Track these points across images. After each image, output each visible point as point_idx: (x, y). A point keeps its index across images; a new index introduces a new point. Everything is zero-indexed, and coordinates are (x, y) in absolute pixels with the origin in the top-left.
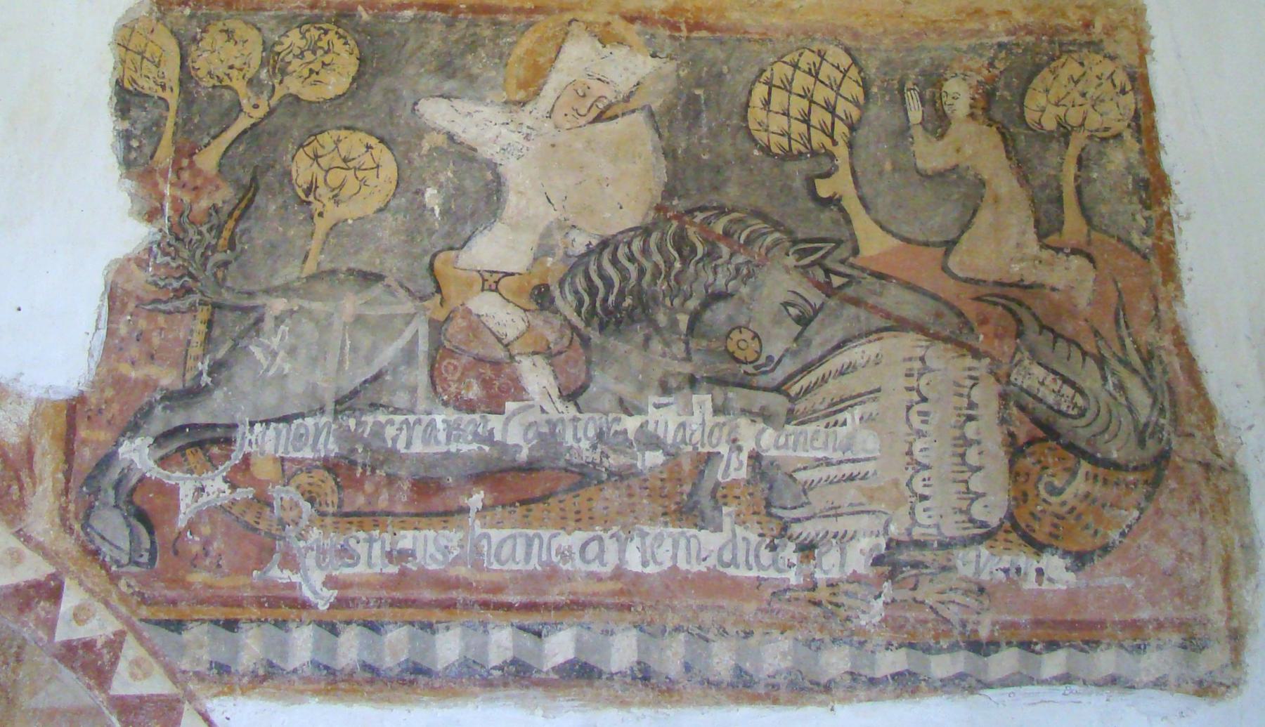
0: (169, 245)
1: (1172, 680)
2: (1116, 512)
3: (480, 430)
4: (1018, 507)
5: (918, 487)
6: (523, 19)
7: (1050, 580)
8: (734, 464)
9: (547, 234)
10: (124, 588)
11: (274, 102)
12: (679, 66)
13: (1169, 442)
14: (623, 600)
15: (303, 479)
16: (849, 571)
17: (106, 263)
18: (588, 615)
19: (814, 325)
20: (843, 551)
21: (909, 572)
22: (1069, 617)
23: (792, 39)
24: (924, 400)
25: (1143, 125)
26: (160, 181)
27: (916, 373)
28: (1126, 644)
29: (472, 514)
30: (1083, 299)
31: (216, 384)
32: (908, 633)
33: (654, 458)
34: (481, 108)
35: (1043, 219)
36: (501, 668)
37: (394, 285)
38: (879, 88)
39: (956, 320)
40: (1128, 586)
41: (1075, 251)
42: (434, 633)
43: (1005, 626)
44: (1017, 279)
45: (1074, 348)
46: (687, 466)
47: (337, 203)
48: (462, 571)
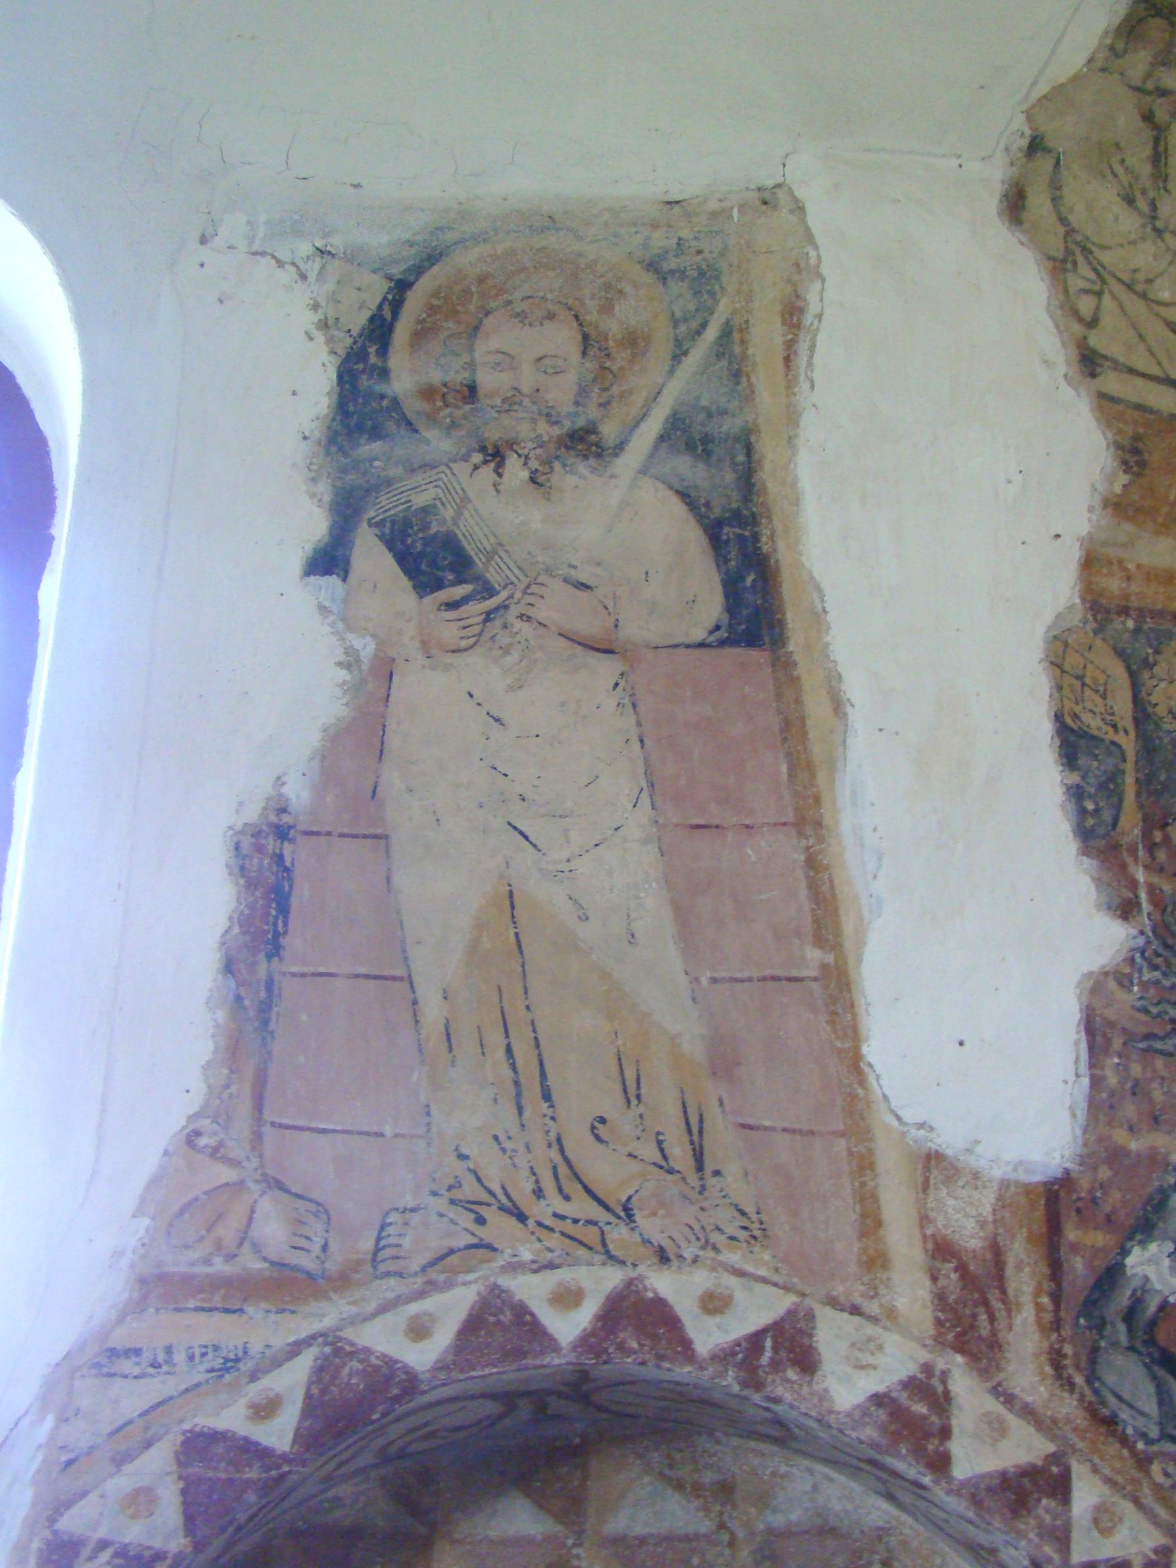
0: (1159, 955)
10: (1160, 1479)
17: (1076, 978)
26: (1129, 860)
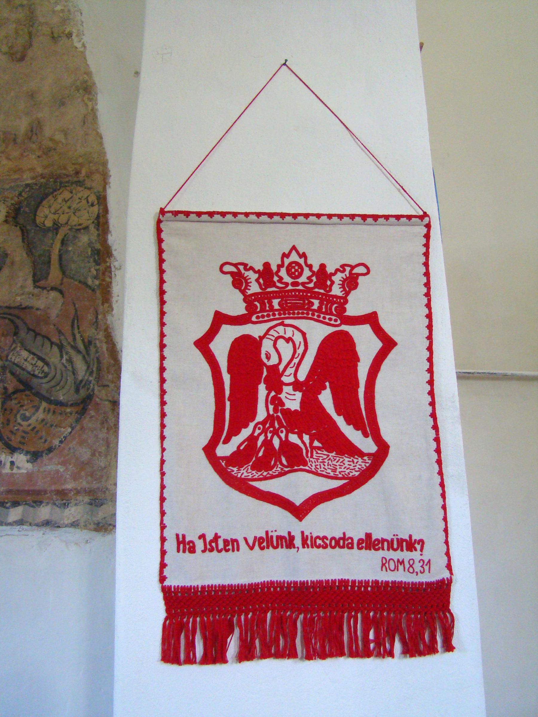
2: (59, 429)
7: (18, 468)
22: (26, 489)
30: (54, 313)
41: (53, 289)
45: (46, 341)
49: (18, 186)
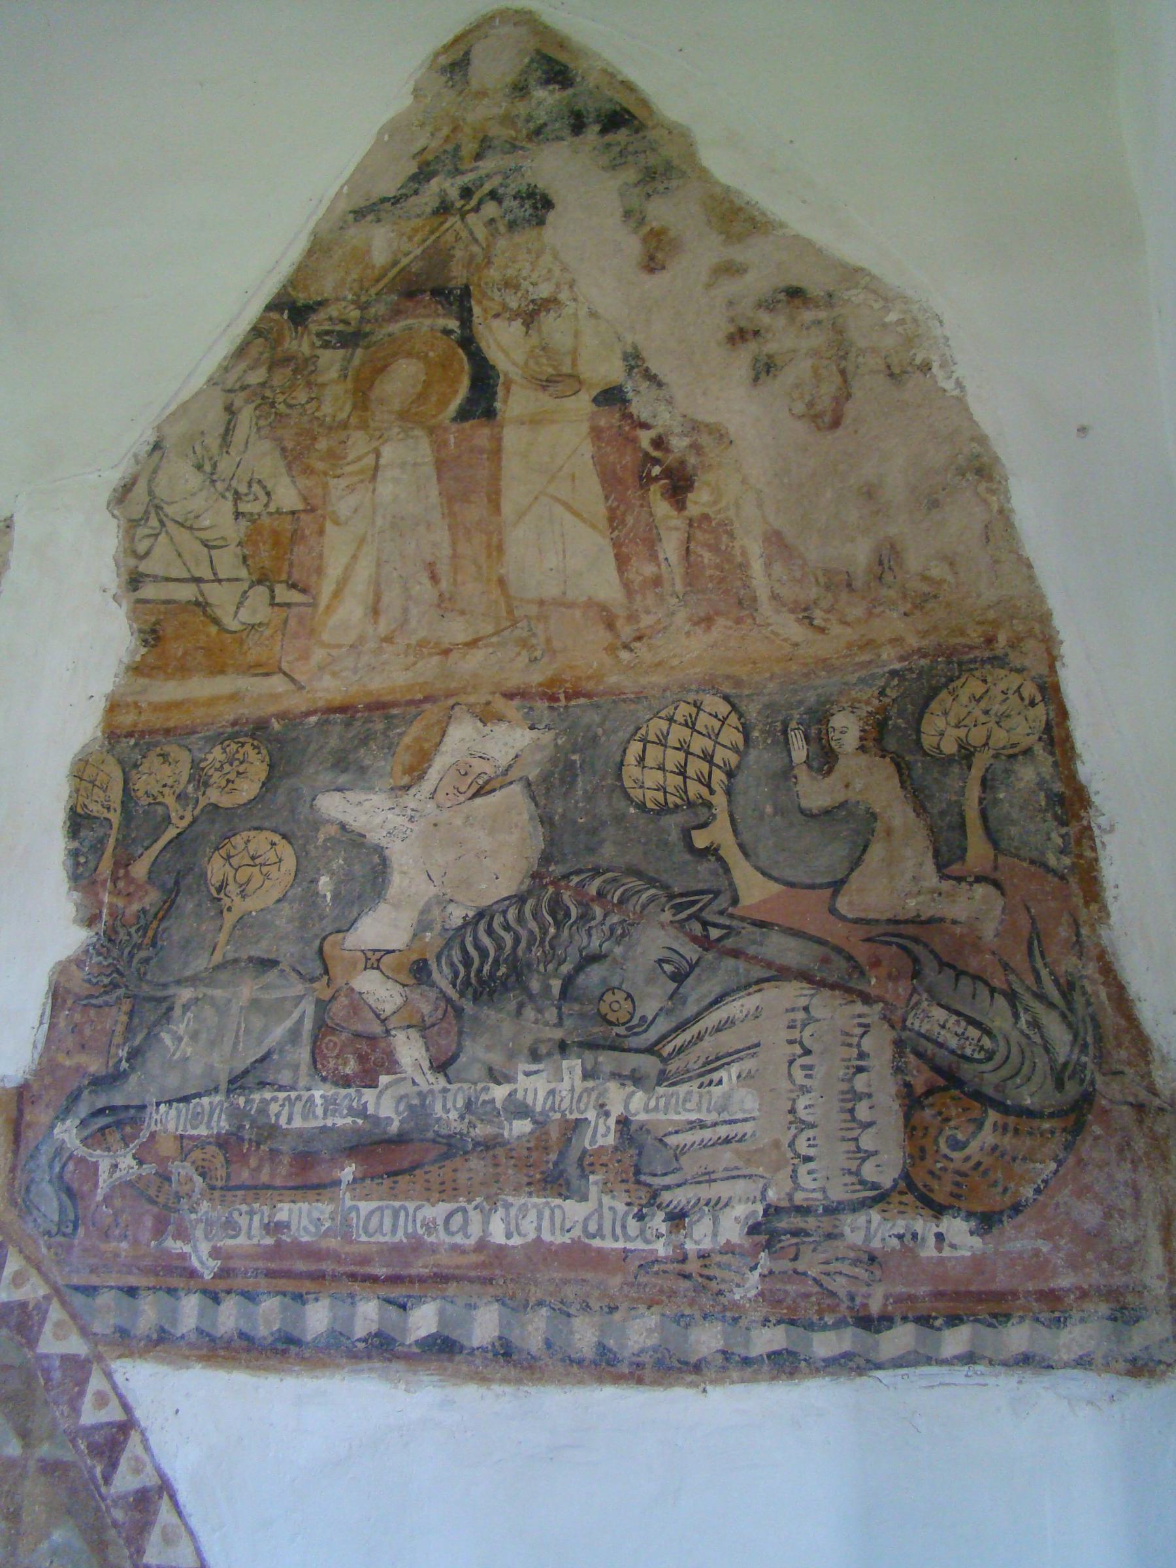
1: (1099, 1360)
3: (355, 1104)
4: (913, 1165)
5: (802, 1148)
6: (413, 710)
7: (953, 1246)
8: (601, 1129)
9: (425, 910)
11: (197, 812)
12: (557, 735)
13: (1092, 1083)
14: (485, 1273)
15: (197, 1154)
16: (722, 1240)
17: (51, 965)
18: (452, 1288)
19: (690, 980)
20: (715, 1221)
21: (787, 1240)
22: (973, 1288)
23: (668, 694)
24: (807, 1052)
25: (1057, 738)
26: (100, 890)
27: (799, 1024)
28: (1042, 1317)
29: (343, 1186)
30: (989, 930)
31: (132, 1068)
32: (788, 1308)
33: (523, 1126)
34: (372, 796)
35: (944, 849)
36: (365, 1340)
37: (288, 969)
38: (762, 732)
39: (844, 964)
40: (1045, 1249)
41: (978, 880)
42: (304, 1303)
43: (900, 1299)
44: (914, 914)
45: (980, 986)
46: (554, 1134)
47: (243, 897)
48: (333, 1243)
49: (873, 676)
